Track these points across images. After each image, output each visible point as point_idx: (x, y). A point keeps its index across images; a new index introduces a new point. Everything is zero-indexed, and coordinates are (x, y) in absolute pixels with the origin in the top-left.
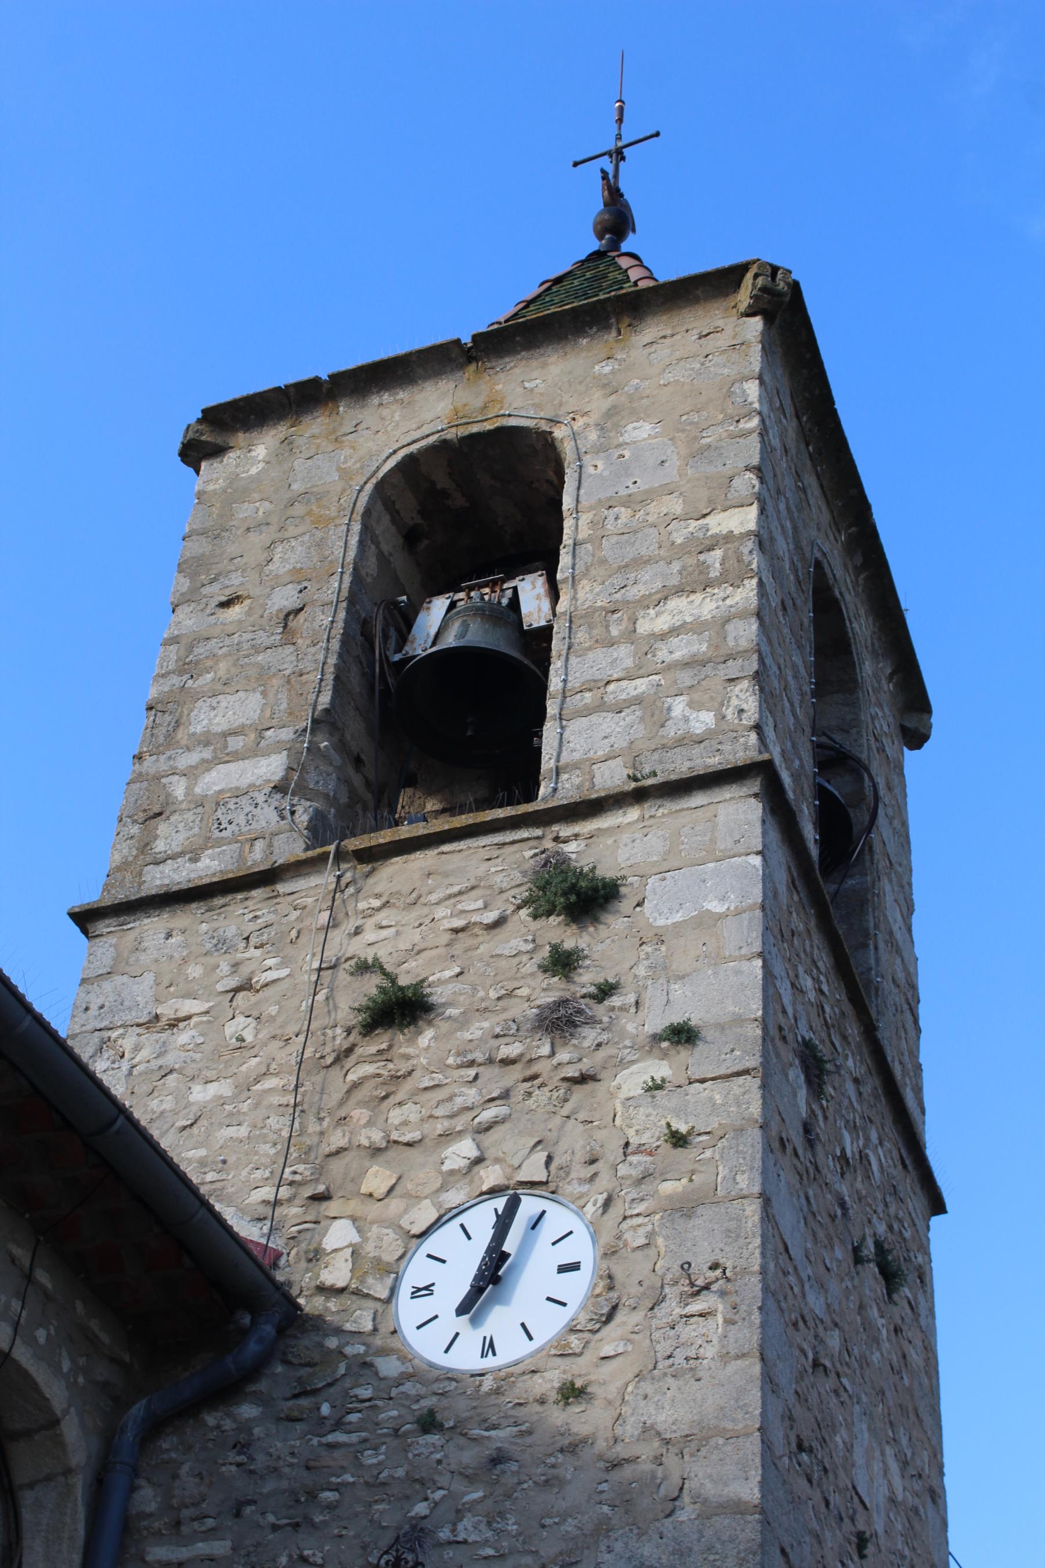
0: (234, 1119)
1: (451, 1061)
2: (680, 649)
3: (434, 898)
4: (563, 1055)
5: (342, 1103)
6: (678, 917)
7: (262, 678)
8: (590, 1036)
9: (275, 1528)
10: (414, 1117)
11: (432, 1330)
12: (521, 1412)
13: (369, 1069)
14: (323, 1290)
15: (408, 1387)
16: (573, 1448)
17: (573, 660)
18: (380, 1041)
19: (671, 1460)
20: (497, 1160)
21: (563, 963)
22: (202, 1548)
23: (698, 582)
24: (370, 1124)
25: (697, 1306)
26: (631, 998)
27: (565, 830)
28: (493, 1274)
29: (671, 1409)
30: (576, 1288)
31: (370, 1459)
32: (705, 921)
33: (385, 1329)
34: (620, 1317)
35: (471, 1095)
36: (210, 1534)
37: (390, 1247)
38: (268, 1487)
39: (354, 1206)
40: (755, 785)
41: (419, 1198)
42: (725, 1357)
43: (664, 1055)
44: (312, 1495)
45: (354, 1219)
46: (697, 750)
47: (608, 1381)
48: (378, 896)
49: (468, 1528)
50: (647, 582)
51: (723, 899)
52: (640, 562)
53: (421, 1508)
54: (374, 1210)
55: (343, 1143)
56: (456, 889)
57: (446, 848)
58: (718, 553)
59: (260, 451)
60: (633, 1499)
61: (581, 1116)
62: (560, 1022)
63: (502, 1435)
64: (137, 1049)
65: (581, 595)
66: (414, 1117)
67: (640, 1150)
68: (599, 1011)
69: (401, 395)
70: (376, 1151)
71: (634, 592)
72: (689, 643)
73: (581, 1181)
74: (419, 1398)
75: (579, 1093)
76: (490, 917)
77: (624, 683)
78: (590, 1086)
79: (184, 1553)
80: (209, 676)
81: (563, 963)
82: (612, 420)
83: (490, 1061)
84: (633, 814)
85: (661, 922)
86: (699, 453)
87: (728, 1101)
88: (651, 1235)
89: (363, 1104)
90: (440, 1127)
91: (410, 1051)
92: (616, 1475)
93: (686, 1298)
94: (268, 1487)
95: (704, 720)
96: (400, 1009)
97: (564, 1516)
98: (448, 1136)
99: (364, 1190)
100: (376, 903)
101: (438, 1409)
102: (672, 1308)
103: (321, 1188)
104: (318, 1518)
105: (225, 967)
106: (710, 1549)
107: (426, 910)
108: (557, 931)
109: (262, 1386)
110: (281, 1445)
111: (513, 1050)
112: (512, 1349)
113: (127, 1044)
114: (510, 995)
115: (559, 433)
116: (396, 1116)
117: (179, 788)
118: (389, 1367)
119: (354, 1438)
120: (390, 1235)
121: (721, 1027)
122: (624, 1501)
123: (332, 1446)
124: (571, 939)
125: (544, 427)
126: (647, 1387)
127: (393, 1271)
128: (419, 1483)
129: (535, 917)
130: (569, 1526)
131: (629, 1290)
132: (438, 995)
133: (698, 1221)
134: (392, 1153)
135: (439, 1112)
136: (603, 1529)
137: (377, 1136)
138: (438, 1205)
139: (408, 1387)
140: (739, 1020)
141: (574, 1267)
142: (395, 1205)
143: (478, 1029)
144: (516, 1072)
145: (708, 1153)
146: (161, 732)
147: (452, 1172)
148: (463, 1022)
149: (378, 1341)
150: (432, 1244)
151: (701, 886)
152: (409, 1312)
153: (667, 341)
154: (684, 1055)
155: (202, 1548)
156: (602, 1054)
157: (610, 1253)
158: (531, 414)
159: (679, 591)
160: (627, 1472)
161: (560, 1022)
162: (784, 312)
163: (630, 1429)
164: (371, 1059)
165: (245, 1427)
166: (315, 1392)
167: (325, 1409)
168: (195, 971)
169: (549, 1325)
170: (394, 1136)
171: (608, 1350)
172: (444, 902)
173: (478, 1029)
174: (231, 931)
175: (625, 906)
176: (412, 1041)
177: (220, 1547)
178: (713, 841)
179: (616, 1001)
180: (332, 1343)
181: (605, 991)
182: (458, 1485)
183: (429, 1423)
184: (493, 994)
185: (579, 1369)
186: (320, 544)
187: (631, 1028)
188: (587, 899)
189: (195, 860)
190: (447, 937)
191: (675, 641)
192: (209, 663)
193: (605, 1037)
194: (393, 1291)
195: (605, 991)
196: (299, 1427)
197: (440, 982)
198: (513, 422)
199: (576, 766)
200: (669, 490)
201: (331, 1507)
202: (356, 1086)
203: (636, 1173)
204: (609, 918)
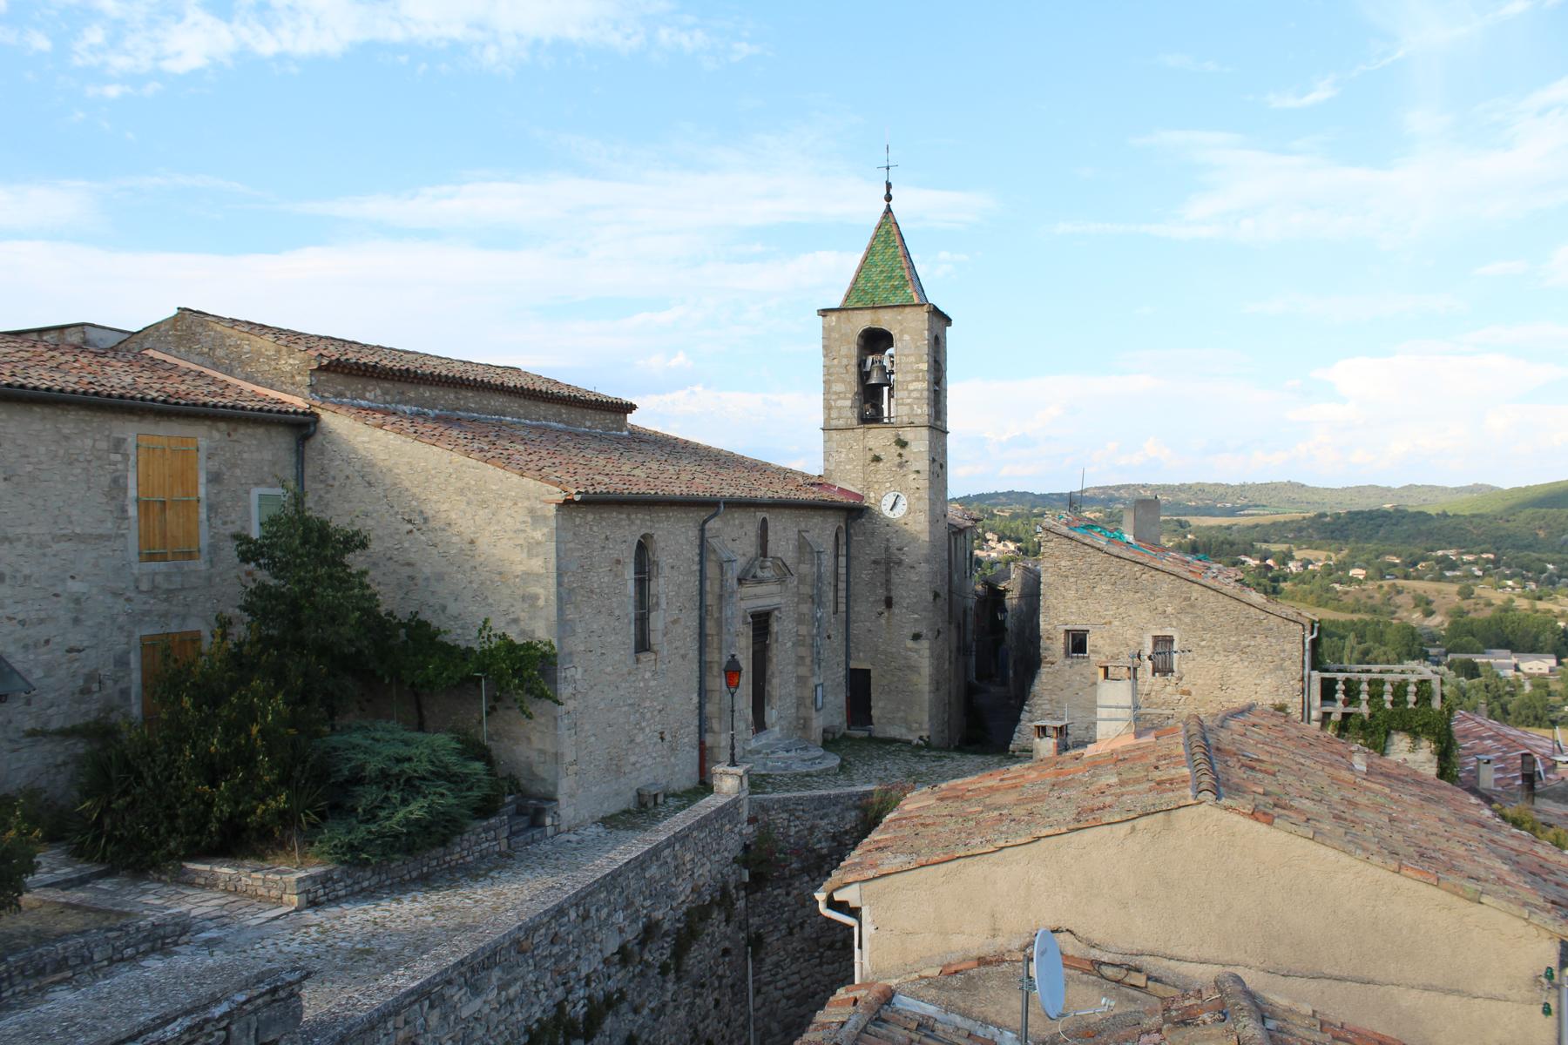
2: (915, 394)
7: (843, 381)
23: (917, 380)
60: (915, 539)
62: (901, 465)
82: (902, 332)
87: (923, 482)
96: (877, 459)
101: (889, 524)
110: (869, 526)
151: (919, 442)
161: (901, 465)
172: (878, 438)
188: (903, 444)
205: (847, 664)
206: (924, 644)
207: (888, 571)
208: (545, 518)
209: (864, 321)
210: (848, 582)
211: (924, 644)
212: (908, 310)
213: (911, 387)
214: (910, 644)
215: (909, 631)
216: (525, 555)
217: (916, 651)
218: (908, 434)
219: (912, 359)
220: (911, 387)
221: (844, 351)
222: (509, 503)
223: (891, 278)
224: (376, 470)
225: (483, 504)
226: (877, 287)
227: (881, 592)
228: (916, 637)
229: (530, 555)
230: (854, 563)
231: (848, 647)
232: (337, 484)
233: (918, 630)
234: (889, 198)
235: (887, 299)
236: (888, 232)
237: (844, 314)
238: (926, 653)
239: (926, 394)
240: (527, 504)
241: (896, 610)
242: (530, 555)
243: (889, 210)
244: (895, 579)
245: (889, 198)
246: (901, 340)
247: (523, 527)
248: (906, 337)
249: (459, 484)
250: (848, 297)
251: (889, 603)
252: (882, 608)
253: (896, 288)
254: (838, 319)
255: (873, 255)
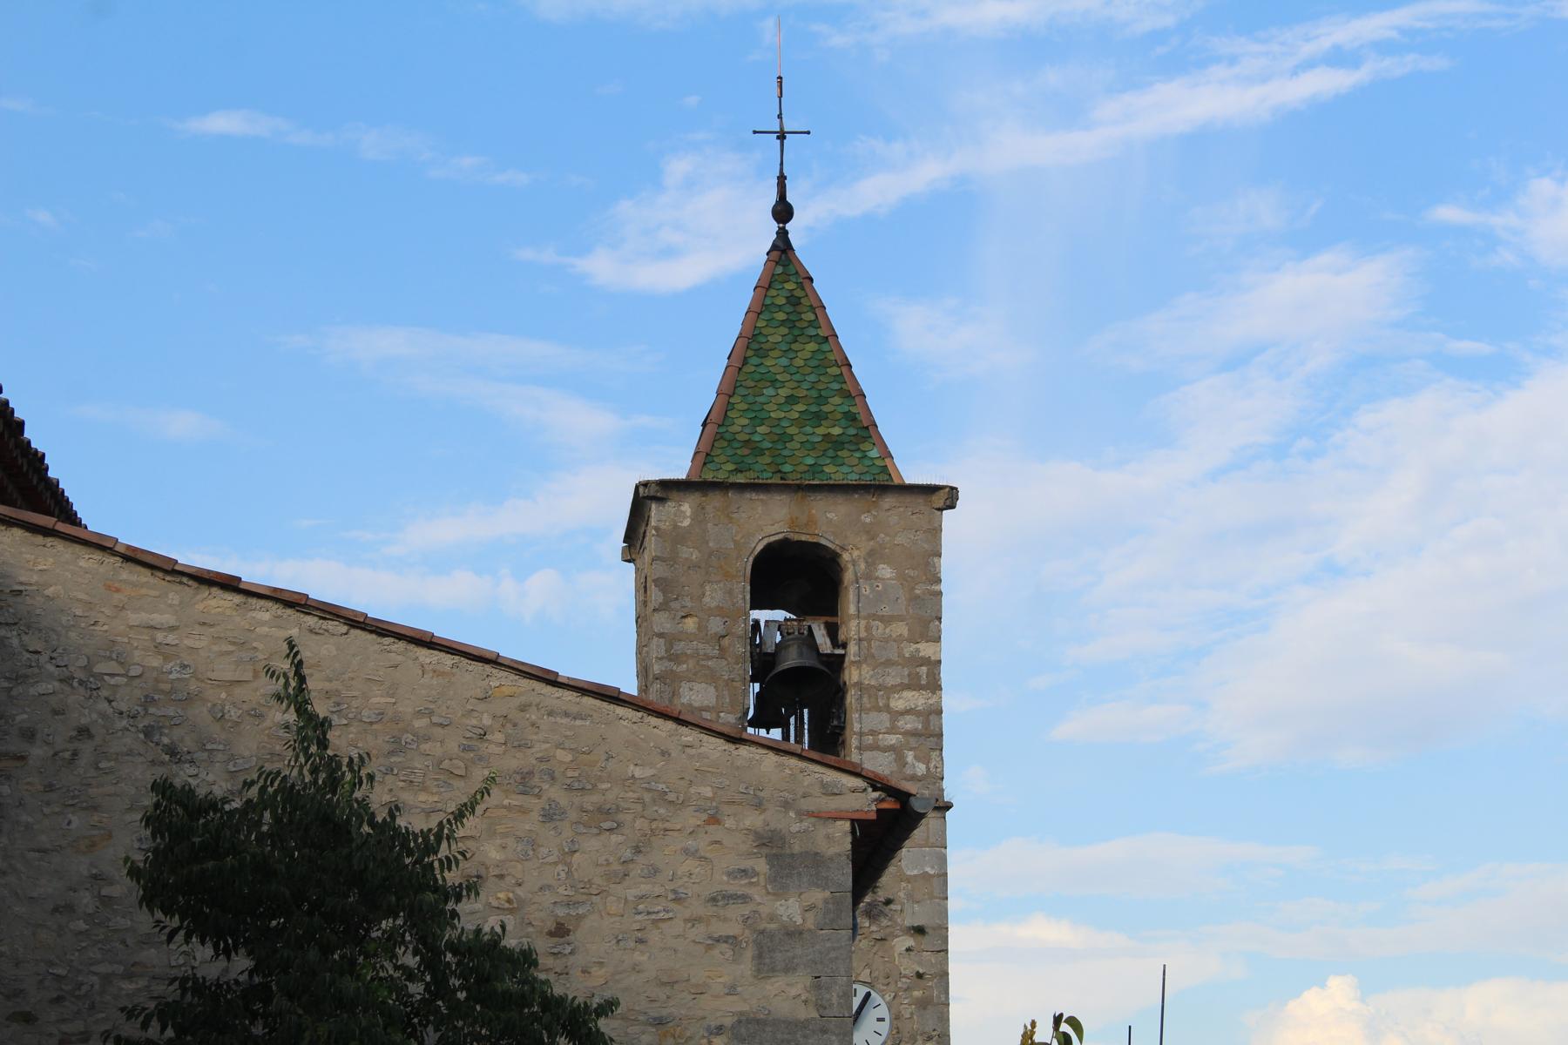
6: (915, 872)
7: (712, 678)
8: (885, 922)
30: (884, 1028)
52: (889, 663)
58: (924, 669)
59: (686, 508)
68: (886, 909)
69: (762, 497)
82: (873, 557)
115: (846, 556)
154: (920, 938)
157: (896, 1017)
159: (909, 687)
179: (892, 906)
181: (888, 902)
186: (730, 592)
195: (888, 902)
198: (823, 542)
200: (900, 618)
208: (816, 861)
209: (768, 520)
212: (889, 501)
213: (898, 703)
216: (746, 967)
219: (901, 629)
220: (898, 703)
221: (713, 596)
222: (690, 819)
223: (819, 418)
224: (200, 713)
225: (605, 818)
226: (784, 438)
229: (765, 967)
232: (37, 752)
234: (783, 212)
235: (815, 469)
236: (794, 301)
237: (715, 501)
240: (753, 820)
242: (765, 967)
243: (782, 248)
245: (783, 212)
246: (869, 577)
247: (738, 886)
248: (885, 571)
249: (513, 762)
250: (704, 456)
253: (836, 444)
254: (699, 511)
255: (762, 353)
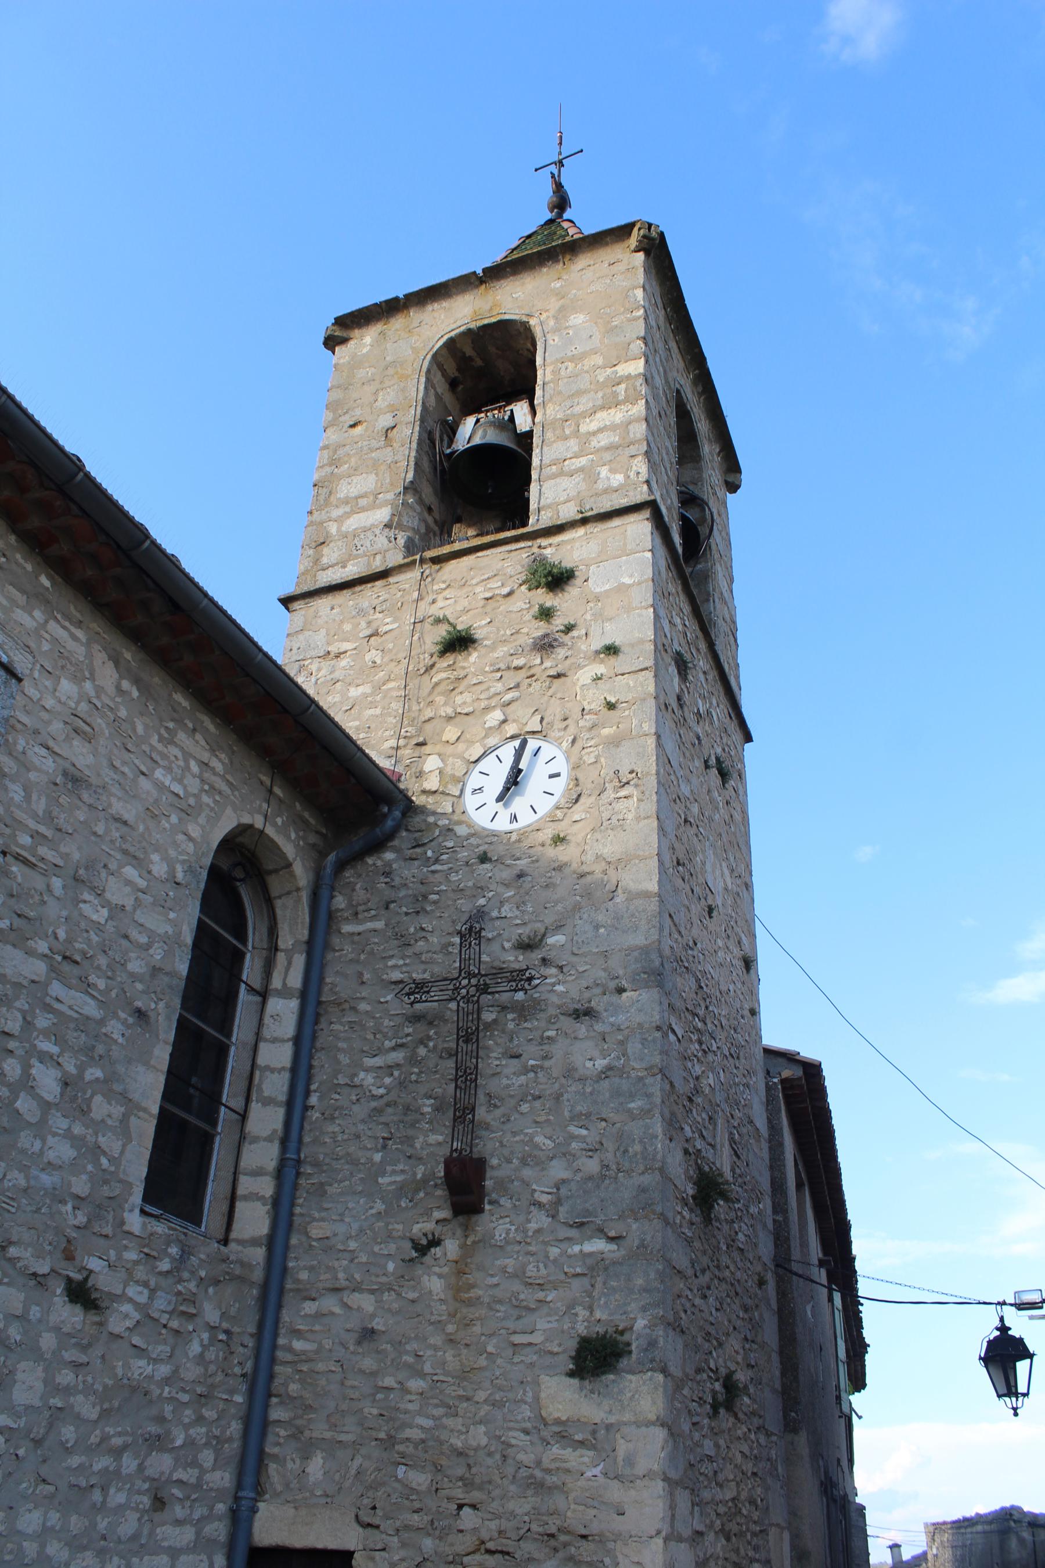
0: (373, 705)
1: (487, 669)
2: (604, 440)
3: (474, 582)
4: (548, 664)
5: (430, 694)
6: (607, 587)
7: (375, 466)
8: (561, 652)
9: (407, 914)
10: (469, 700)
11: (482, 810)
12: (532, 851)
13: (443, 675)
14: (424, 792)
15: (472, 840)
16: (560, 868)
17: (545, 448)
18: (450, 659)
19: (611, 872)
20: (514, 721)
21: (546, 614)
22: (370, 925)
23: (612, 403)
24: (445, 704)
25: (623, 793)
26: (584, 632)
27: (544, 542)
28: (514, 780)
29: (610, 846)
30: (559, 786)
31: (454, 877)
32: (622, 589)
33: (458, 811)
34: (582, 800)
35: (499, 687)
36: (373, 918)
37: (457, 767)
38: (402, 894)
39: (439, 748)
40: (647, 513)
41: (473, 743)
42: (638, 819)
43: (602, 661)
44: (425, 897)
45: (440, 755)
46: (615, 495)
47: (577, 833)
48: (444, 582)
49: (506, 911)
50: (584, 404)
51: (631, 576)
53: (482, 901)
54: (450, 749)
55: (431, 715)
56: (486, 576)
57: (480, 554)
58: (623, 386)
59: (368, 340)
60: (592, 892)
61: (559, 696)
62: (545, 646)
63: (522, 863)
64: (319, 670)
65: (548, 412)
66: (469, 700)
67: (590, 712)
68: (566, 639)
70: (450, 718)
71: (578, 409)
72: (608, 437)
73: (559, 730)
74: (478, 846)
75: (557, 682)
76: (505, 590)
77: (574, 460)
78: (563, 679)
79: (360, 928)
80: (346, 466)
81: (546, 614)
82: (562, 314)
83: (509, 668)
84: (581, 531)
85: (598, 590)
86: (610, 331)
87: (637, 685)
88: (597, 757)
89: (439, 694)
90: (483, 705)
91: (466, 664)
92: (583, 881)
93: (616, 790)
94: (402, 894)
95: (618, 479)
96: (459, 642)
97: (556, 903)
98: (487, 709)
99: (444, 739)
100: (443, 586)
101: (487, 852)
102: (610, 794)
103: (421, 739)
104: (428, 909)
105: (363, 624)
106: (633, 915)
107: (470, 588)
108: (543, 597)
109: (396, 843)
110: (408, 873)
111: (520, 662)
112: (527, 818)
113: (314, 668)
114: (518, 632)
115: (532, 322)
116: (459, 700)
117: (333, 528)
118: (461, 830)
119: (445, 867)
120: (459, 762)
121: (632, 646)
122: (588, 894)
123: (433, 872)
124: (548, 599)
125: (525, 319)
126: (598, 835)
127: (461, 781)
128: (480, 889)
129: (530, 590)
130: (559, 907)
131: (587, 786)
132: (478, 634)
133: (621, 749)
134: (458, 719)
135: (482, 697)
136: (577, 908)
137: (450, 711)
138: (484, 746)
139: (472, 840)
140: (641, 641)
141: (558, 775)
142: (461, 746)
143: (501, 651)
144: (523, 674)
145: (627, 713)
146: (322, 498)
147: (490, 728)
148: (493, 648)
149: (455, 817)
150: (482, 766)
151: (620, 571)
152: (470, 802)
153: (592, 268)
154: (612, 660)
155: (370, 925)
156: (568, 662)
157: (576, 767)
158: (517, 312)
159: (602, 408)
160: (589, 878)
161: (545, 646)
162: (657, 251)
163: (589, 857)
164: (445, 670)
165: (389, 864)
166: (424, 845)
167: (429, 853)
168: (347, 627)
169: (545, 806)
170: (459, 710)
171: (577, 817)
172: (481, 582)
173: (501, 651)
174: (366, 604)
175: (578, 581)
176: (466, 659)
177: (379, 925)
178: (625, 544)
179: (574, 633)
180: (431, 819)
181: (569, 628)
182: (501, 889)
183: (484, 858)
184: (508, 632)
185: (562, 828)
186: (403, 390)
187: (583, 647)
188: (558, 579)
189: (344, 567)
190: (483, 602)
191: (600, 436)
192: (346, 459)
193: (569, 653)
194: (462, 791)
195: (569, 628)
196: (416, 863)
197: (480, 627)
198: (507, 317)
199: (549, 506)
201: (435, 902)
202: (437, 684)
203: (588, 724)
204: (568, 588)
205: (240, 1517)
206: (640, 1396)
207: (470, 1036)
210: (295, 1105)
211: (640, 1396)
214: (563, 1397)
215: (554, 1330)
217: (595, 1439)
218: (568, 550)
220: (589, 426)
227: (435, 1141)
228: (597, 1358)
230: (335, 1028)
231: (256, 1425)
233: (598, 1317)
238: (650, 1449)
239: (640, 430)
241: (497, 1223)
244: (502, 1074)
251: (465, 1187)
252: (433, 1215)
